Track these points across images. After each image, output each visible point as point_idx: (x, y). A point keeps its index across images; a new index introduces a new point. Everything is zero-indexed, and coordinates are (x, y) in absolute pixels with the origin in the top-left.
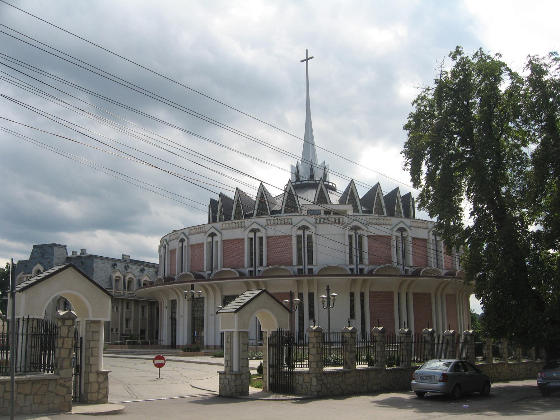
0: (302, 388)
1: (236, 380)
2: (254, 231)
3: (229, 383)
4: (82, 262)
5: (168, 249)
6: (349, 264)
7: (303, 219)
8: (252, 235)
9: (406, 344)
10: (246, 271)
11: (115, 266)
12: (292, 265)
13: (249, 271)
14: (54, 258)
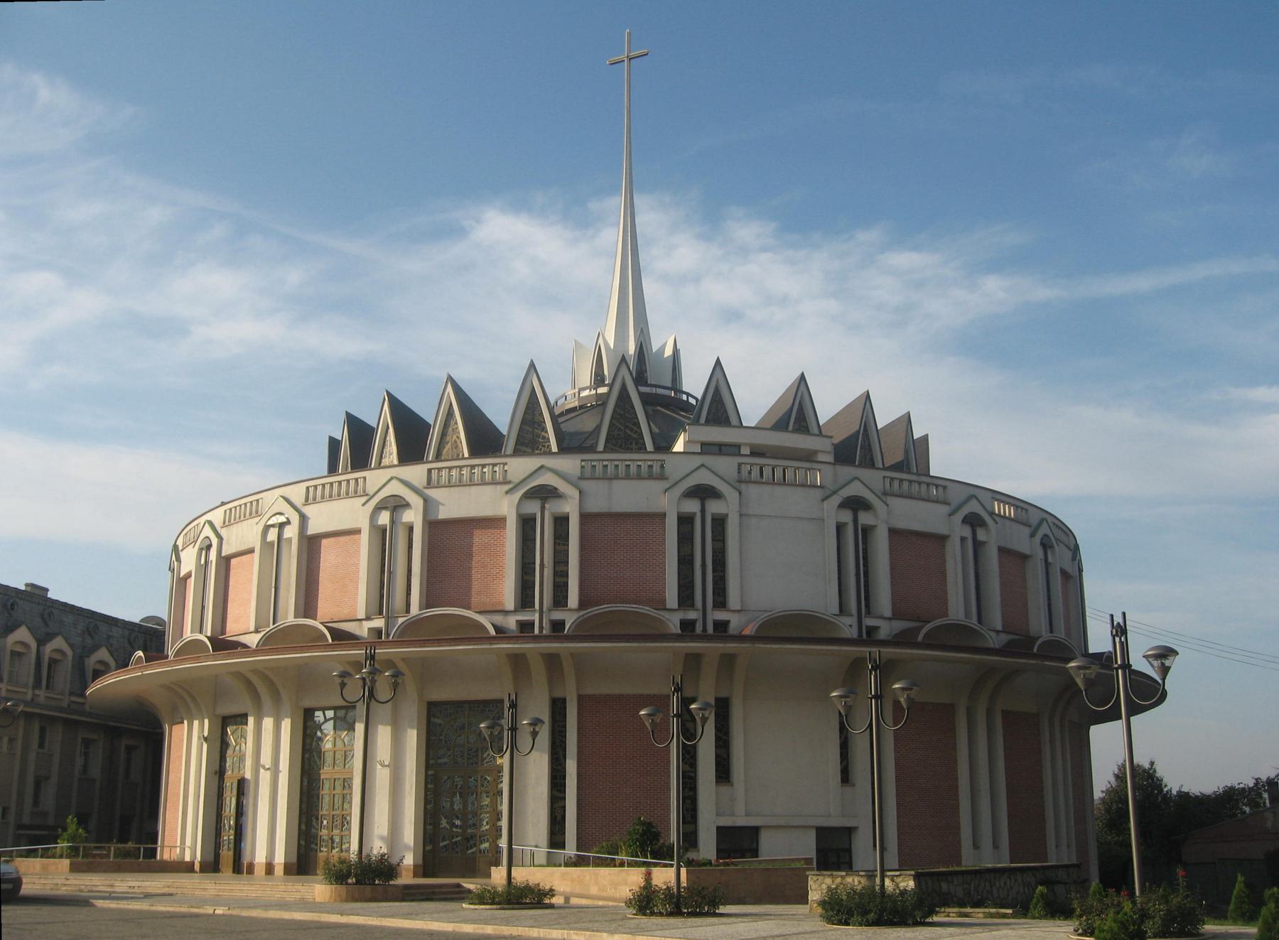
12: (666, 609)
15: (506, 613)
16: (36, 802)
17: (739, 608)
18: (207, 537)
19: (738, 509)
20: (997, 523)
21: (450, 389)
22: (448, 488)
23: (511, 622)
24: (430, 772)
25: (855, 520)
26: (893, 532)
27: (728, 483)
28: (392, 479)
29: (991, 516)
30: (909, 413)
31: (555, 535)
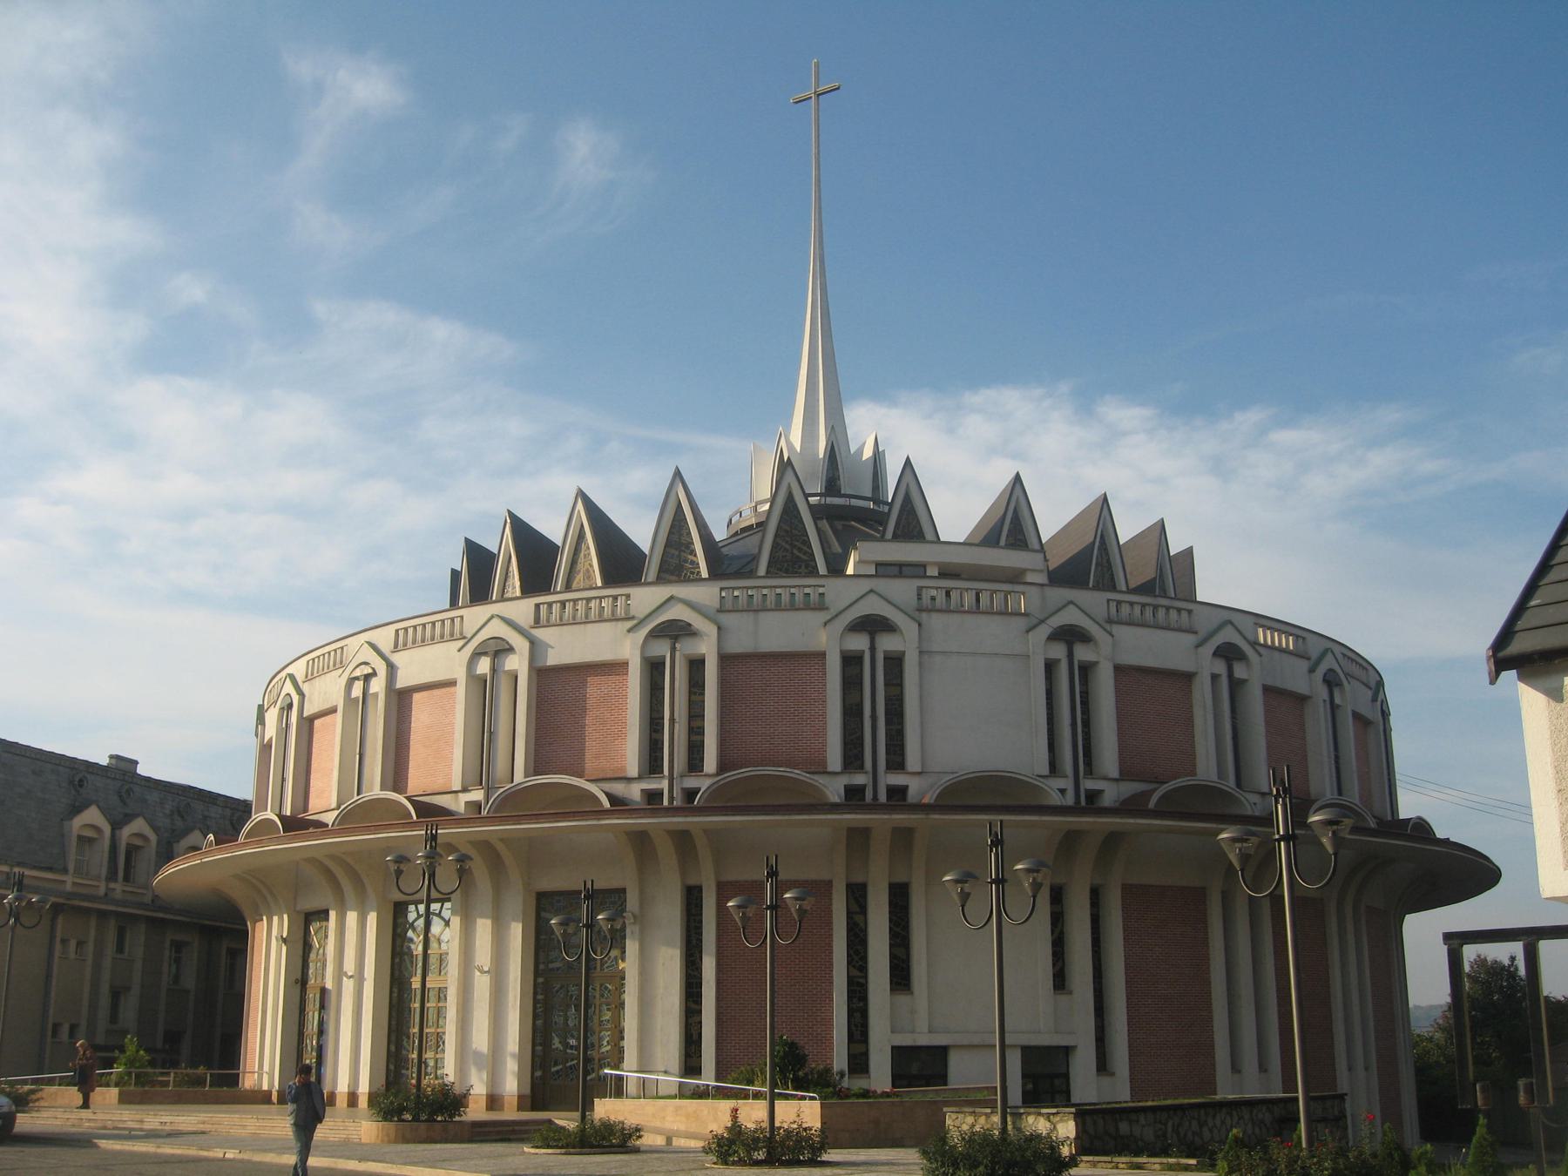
7: (871, 591)
15: (629, 780)
16: (114, 1018)
17: (920, 770)
18: (288, 694)
19: (917, 645)
20: (1260, 655)
21: (580, 506)
22: (560, 627)
23: (635, 792)
24: (541, 980)
25: (1070, 655)
26: (1119, 670)
27: (906, 613)
28: (492, 617)
29: (1254, 648)
30: (1162, 519)
31: (690, 682)
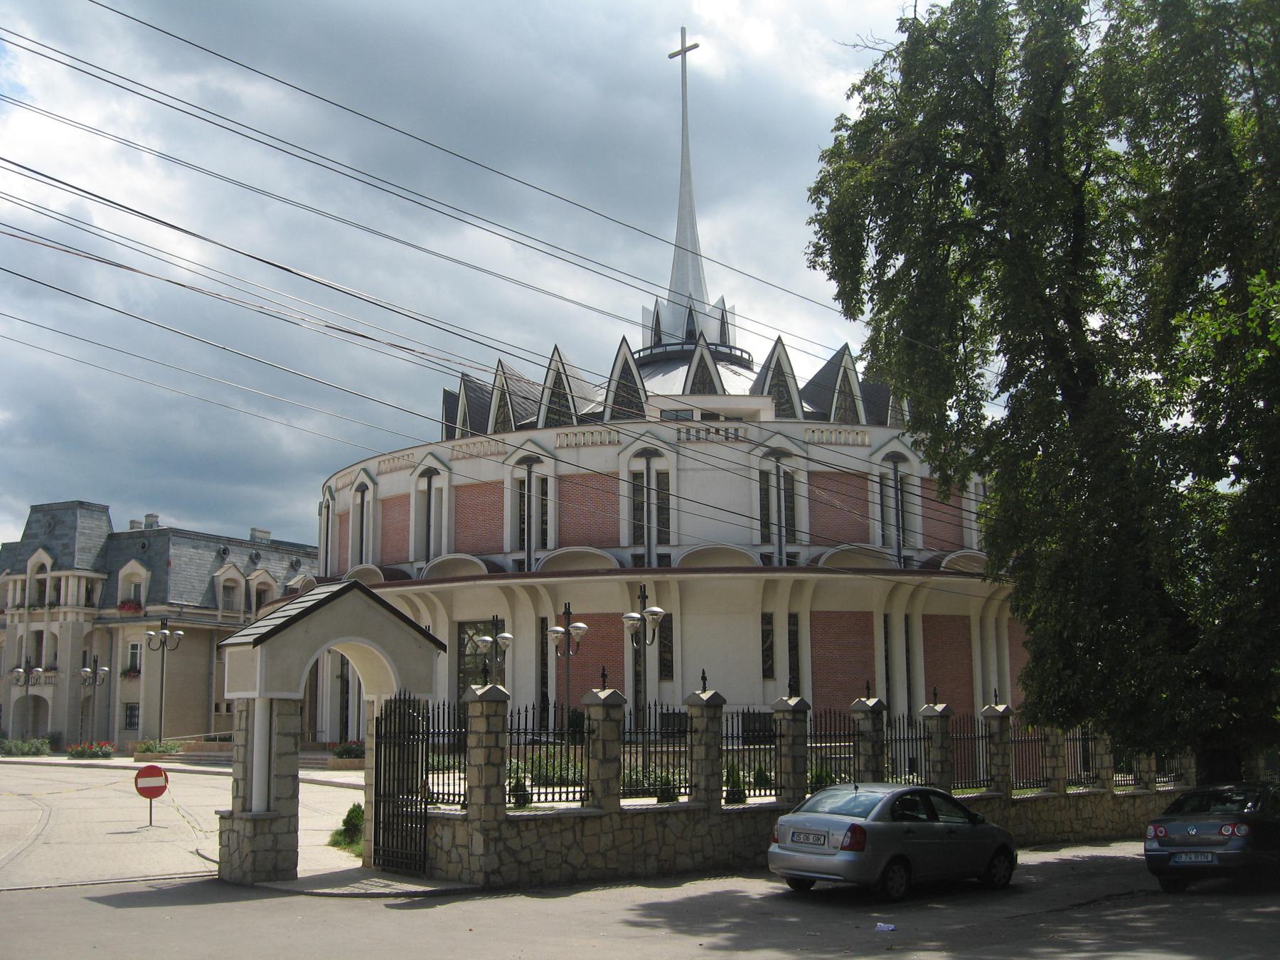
0: (449, 862)
1: (255, 835)
2: (529, 461)
3: (238, 845)
4: (144, 544)
5: (333, 511)
6: (760, 543)
7: (647, 432)
8: (522, 473)
9: (790, 739)
10: (508, 560)
11: (225, 554)
12: (619, 547)
13: (514, 560)
14: (77, 534)
19: (675, 465)
